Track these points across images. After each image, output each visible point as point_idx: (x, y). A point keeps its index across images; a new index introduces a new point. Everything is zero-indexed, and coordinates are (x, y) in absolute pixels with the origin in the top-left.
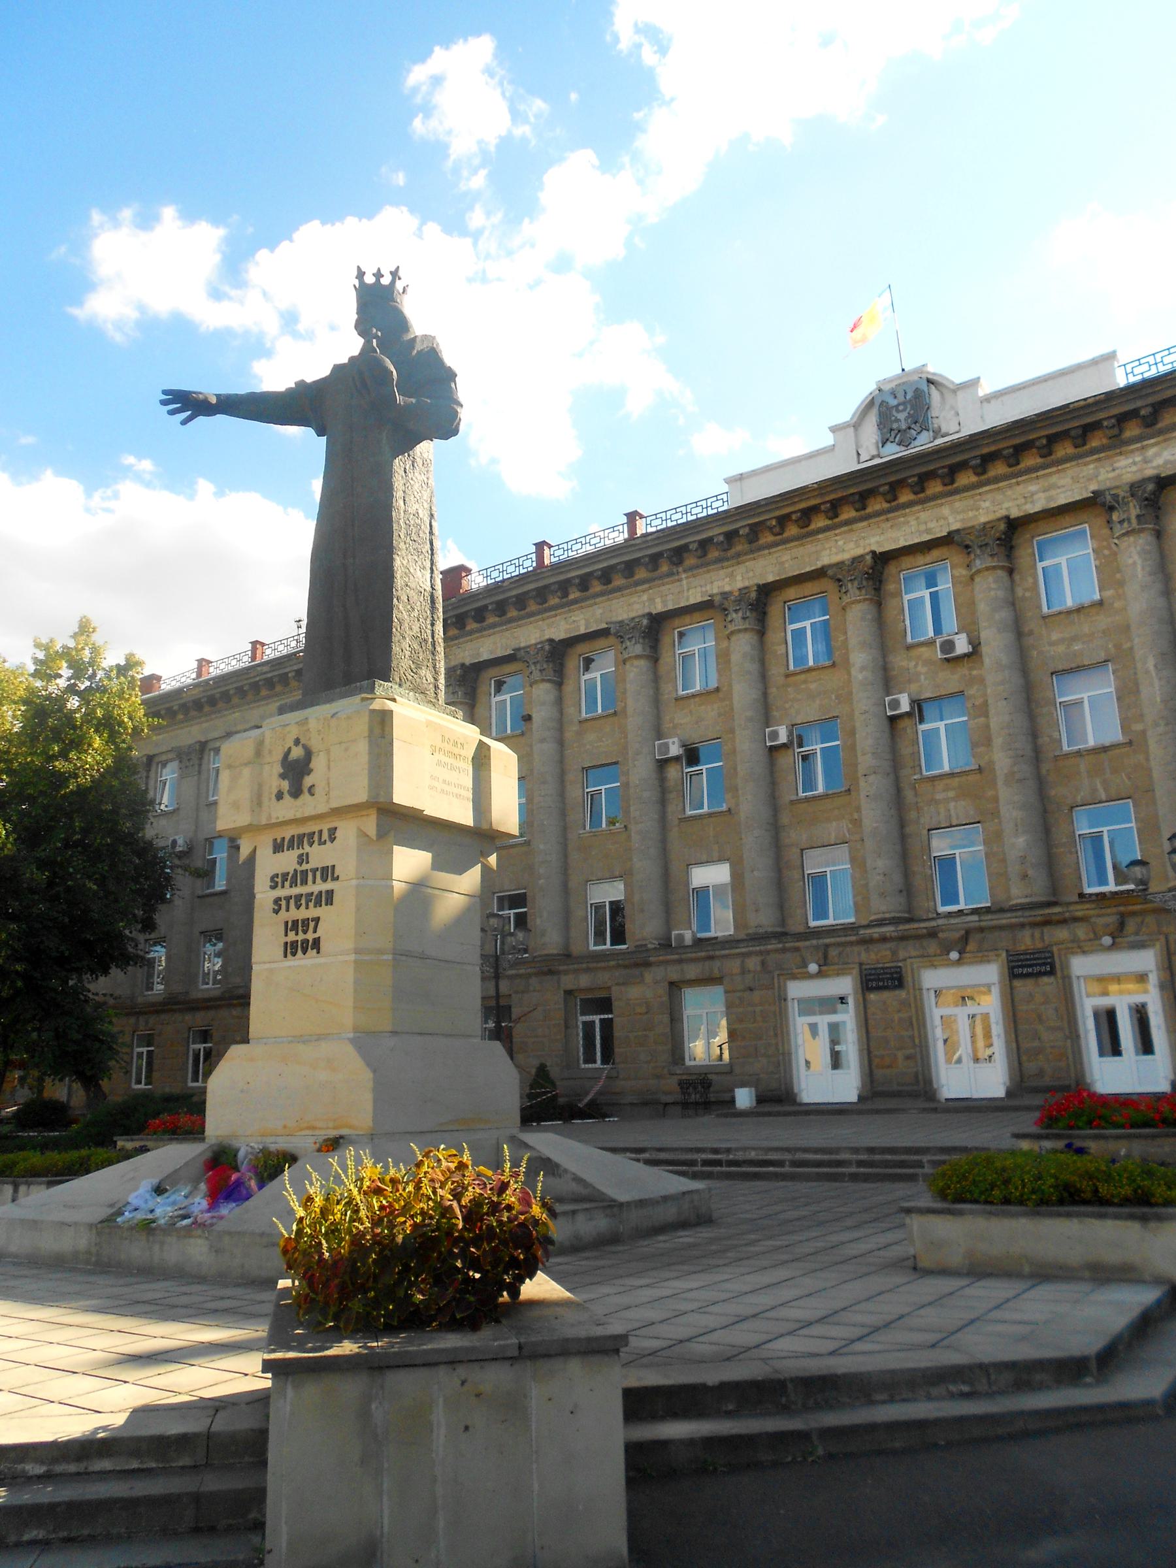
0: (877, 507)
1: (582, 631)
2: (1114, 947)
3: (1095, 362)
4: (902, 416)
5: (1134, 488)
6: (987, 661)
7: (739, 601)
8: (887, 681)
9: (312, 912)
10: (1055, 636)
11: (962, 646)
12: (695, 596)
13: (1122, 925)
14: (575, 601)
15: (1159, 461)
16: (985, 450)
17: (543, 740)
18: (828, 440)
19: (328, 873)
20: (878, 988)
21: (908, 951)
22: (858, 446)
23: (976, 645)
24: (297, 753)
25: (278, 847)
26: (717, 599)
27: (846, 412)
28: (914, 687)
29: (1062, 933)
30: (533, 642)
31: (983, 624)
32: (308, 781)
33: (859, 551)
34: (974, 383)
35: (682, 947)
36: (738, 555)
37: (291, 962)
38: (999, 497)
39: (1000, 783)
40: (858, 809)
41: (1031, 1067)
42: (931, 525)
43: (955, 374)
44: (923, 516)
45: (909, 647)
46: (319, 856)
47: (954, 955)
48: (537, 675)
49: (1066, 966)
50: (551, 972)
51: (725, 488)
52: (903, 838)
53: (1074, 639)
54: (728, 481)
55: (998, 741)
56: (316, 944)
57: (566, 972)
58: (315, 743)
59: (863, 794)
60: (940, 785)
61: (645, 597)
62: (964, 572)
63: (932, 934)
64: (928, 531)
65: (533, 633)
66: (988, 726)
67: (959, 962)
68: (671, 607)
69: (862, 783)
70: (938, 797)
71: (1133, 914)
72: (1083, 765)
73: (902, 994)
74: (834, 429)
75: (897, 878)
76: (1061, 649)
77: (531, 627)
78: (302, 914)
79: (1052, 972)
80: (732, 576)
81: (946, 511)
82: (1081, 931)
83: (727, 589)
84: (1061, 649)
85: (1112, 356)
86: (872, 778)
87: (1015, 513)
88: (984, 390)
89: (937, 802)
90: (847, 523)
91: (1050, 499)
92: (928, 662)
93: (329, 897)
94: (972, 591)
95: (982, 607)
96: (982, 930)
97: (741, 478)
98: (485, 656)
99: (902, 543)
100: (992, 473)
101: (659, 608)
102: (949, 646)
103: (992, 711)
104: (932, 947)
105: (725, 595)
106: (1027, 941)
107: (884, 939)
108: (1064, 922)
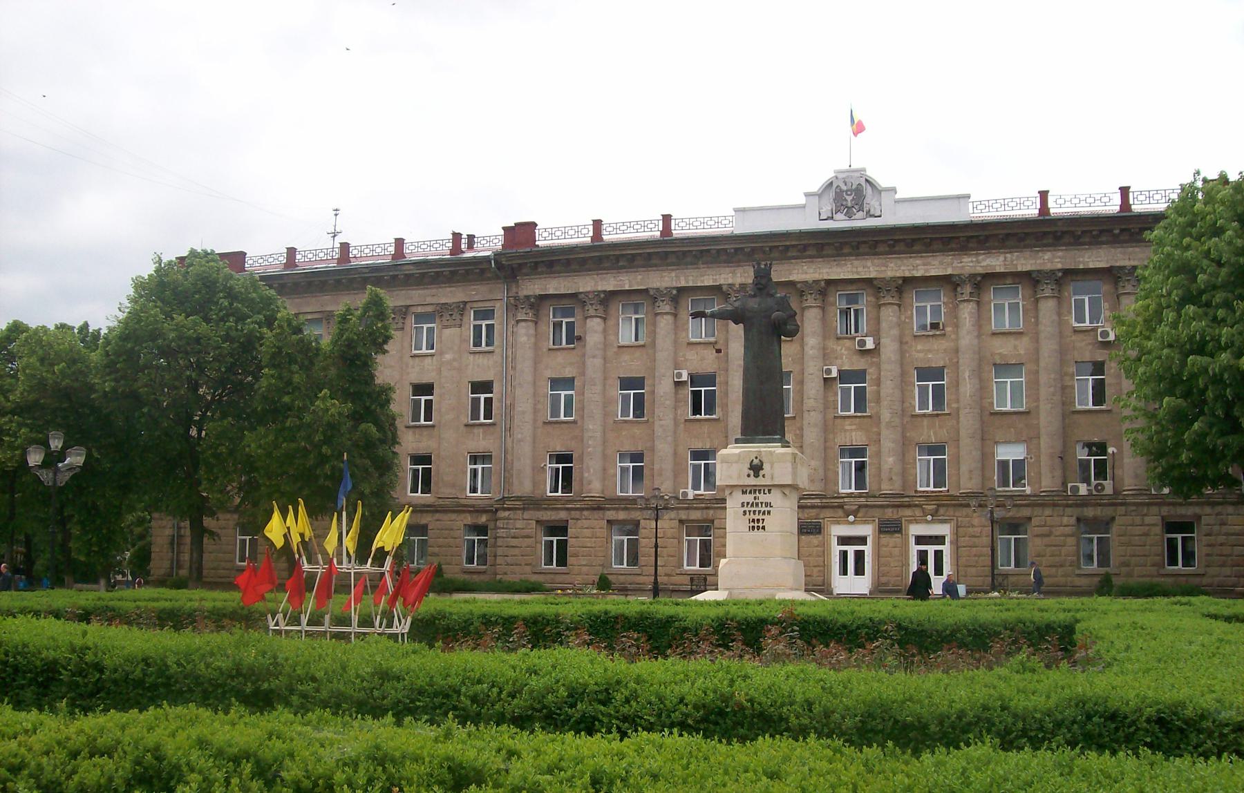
0: (830, 252)
1: (627, 288)
2: (932, 521)
3: (959, 197)
4: (849, 198)
5: (973, 276)
6: (883, 356)
7: (738, 291)
8: (826, 356)
9: (761, 517)
10: (919, 347)
11: (870, 344)
12: (708, 281)
13: (937, 511)
14: (623, 267)
15: (984, 264)
16: (897, 238)
17: (594, 357)
18: (802, 201)
19: (767, 505)
20: (807, 533)
21: (828, 513)
22: (820, 208)
23: (877, 344)
24: (756, 462)
25: (744, 492)
26: (725, 288)
27: (815, 187)
28: (839, 362)
29: (908, 512)
30: (589, 289)
31: (883, 334)
32: (761, 473)
33: (817, 276)
34: (894, 190)
35: (685, 500)
36: (739, 261)
37: (752, 533)
38: (899, 262)
39: (883, 425)
40: (801, 429)
41: (884, 580)
42: (860, 269)
43: (883, 182)
44: (856, 263)
45: (838, 339)
46: (763, 498)
47: (851, 518)
48: (592, 312)
49: (907, 529)
50: (599, 508)
51: (733, 213)
52: (825, 449)
53: (929, 351)
54: (736, 210)
55: (885, 403)
56: (763, 528)
57: (609, 509)
58: (764, 460)
59: (805, 422)
60: (848, 422)
61: (673, 274)
62: (872, 299)
63: (841, 506)
64: (858, 273)
65: (587, 284)
66: (879, 392)
67: (852, 523)
68: (691, 284)
69: (806, 415)
70: (848, 427)
71: (943, 505)
72: (925, 421)
73: (820, 537)
74: (807, 195)
75: (821, 472)
76: (921, 355)
77: (588, 278)
78: (756, 517)
79: (900, 531)
80: (734, 273)
81: (869, 263)
82: (918, 512)
83: (730, 281)
84: (921, 355)
85: (968, 197)
86: (812, 413)
87: (907, 274)
88: (898, 196)
89: (846, 431)
90: (810, 257)
91: (926, 271)
92: (848, 349)
93: (769, 512)
94: (879, 312)
95: (884, 325)
96: (866, 506)
97: (743, 210)
98: (551, 292)
99: (842, 277)
100: (897, 249)
101: (683, 284)
102: (862, 343)
103: (883, 386)
104: (840, 512)
105: (731, 286)
106: (890, 514)
107: (813, 507)
108: (909, 506)
